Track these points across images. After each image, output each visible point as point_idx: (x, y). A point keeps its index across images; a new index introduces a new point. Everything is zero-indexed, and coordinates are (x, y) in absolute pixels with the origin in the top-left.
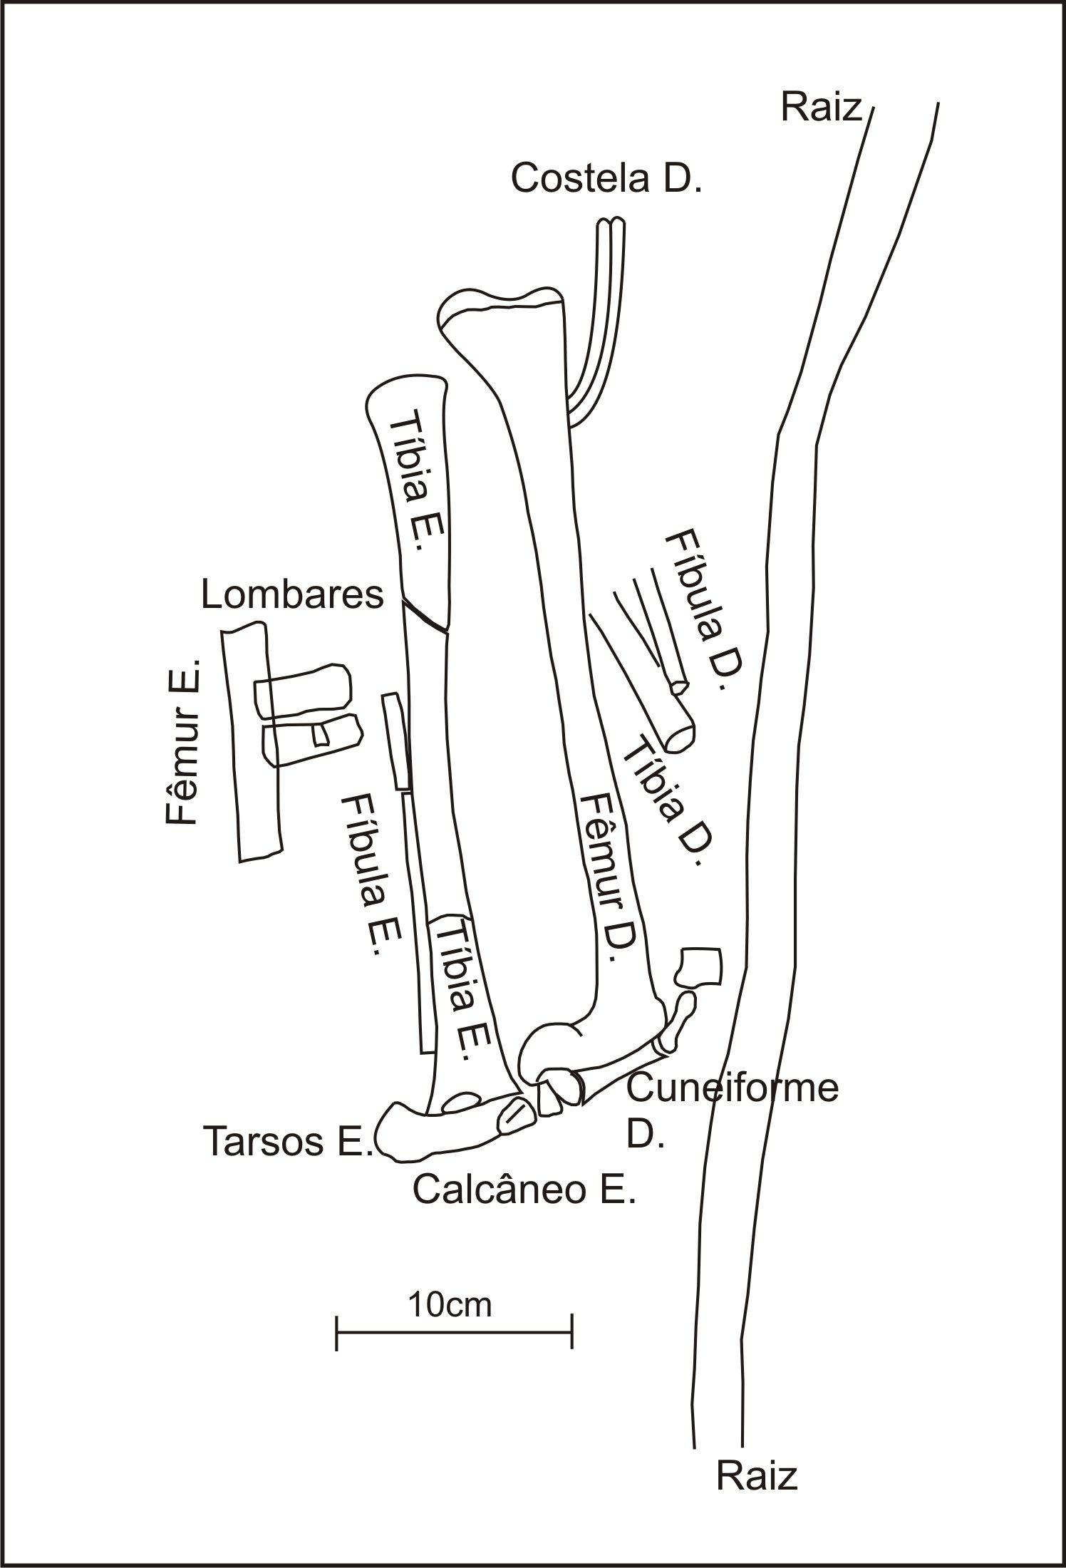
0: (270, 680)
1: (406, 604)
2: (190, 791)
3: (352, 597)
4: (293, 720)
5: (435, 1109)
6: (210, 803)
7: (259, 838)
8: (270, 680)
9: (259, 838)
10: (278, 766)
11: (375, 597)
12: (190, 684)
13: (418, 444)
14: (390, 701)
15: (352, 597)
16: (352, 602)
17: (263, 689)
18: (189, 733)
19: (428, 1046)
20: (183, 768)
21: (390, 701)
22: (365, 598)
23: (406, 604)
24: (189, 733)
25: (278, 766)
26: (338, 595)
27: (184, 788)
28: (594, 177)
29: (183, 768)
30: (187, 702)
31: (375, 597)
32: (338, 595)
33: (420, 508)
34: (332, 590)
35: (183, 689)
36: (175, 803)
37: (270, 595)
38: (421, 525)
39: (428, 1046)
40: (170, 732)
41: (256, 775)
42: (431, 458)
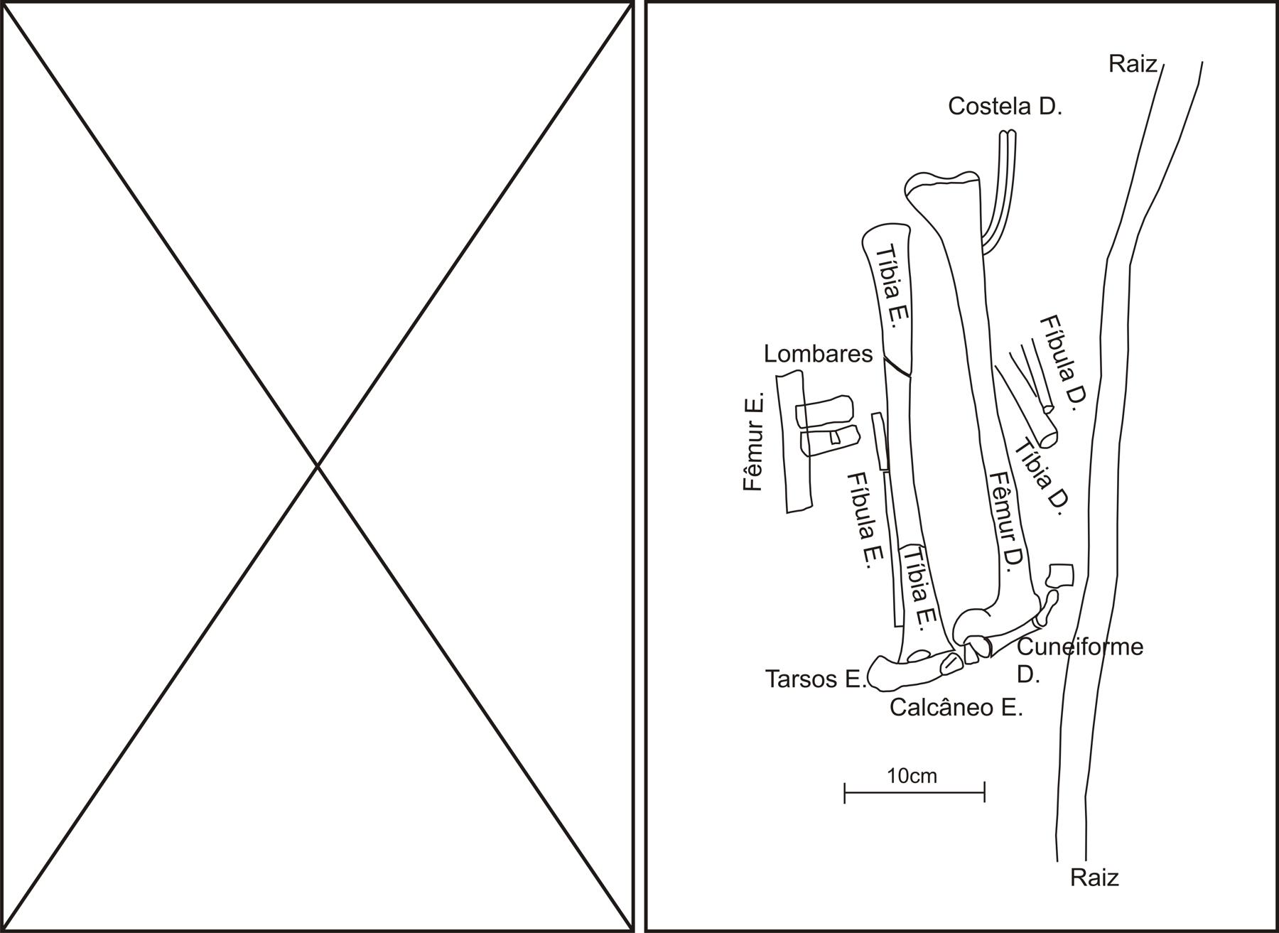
0: (805, 405)
1: (886, 359)
2: (758, 471)
3: (854, 355)
4: (819, 429)
5: (903, 660)
6: (770, 478)
7: (799, 498)
8: (805, 405)
9: (799, 498)
10: (810, 456)
11: (867, 356)
12: (758, 407)
13: (893, 265)
14: (877, 418)
15: (854, 355)
16: (854, 358)
17: (801, 410)
18: (757, 436)
19: (899, 622)
20: (753, 457)
21: (877, 418)
22: (862, 356)
23: (886, 359)
24: (757, 436)
25: (810, 456)
26: (846, 354)
27: (754, 469)
28: (998, 106)
29: (753, 457)
30: (756, 418)
31: (867, 356)
32: (846, 354)
33: (895, 302)
34: (842, 352)
35: (753, 410)
36: (749, 478)
37: (805, 354)
38: (895, 313)
39: (899, 622)
40: (746, 436)
41: (797, 462)
42: (901, 273)
